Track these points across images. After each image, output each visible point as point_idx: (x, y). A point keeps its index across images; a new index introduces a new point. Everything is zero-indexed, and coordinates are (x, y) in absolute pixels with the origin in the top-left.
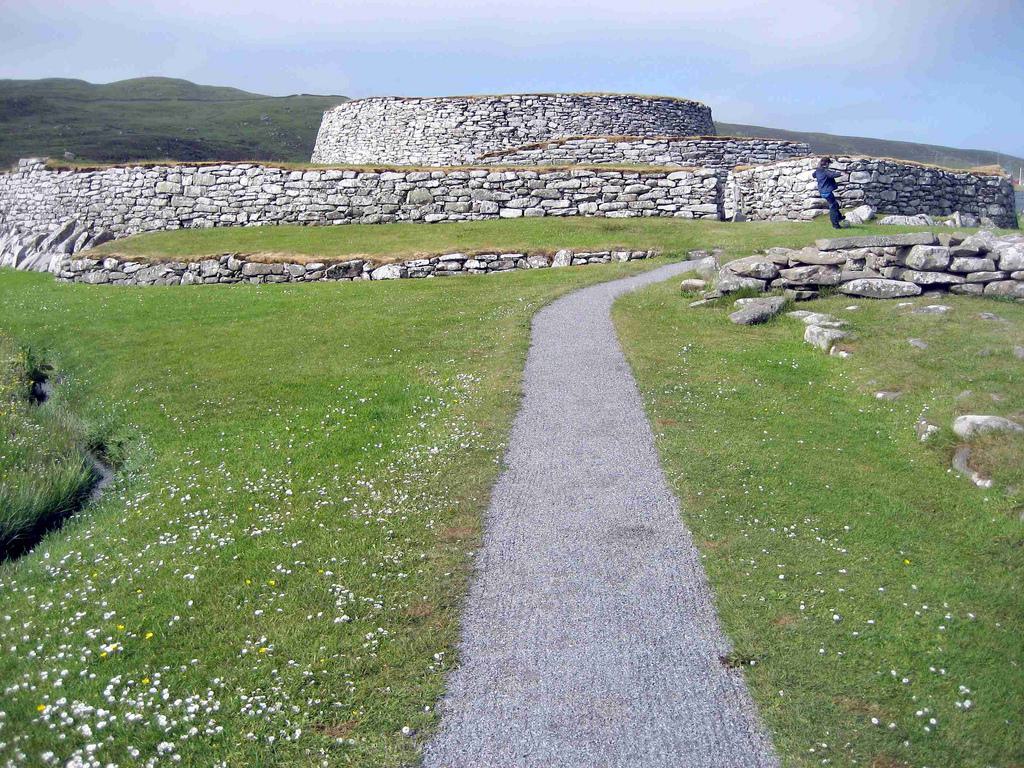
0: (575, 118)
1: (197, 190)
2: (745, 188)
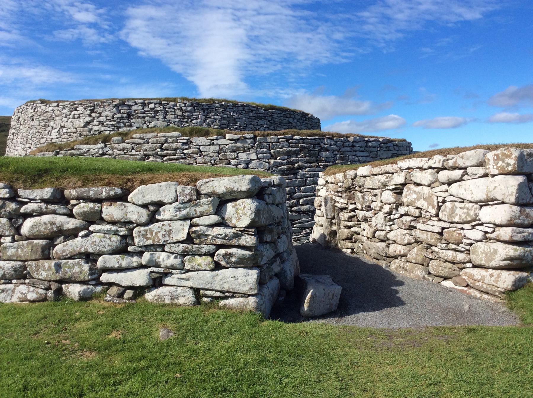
0: (193, 122)
2: (342, 201)
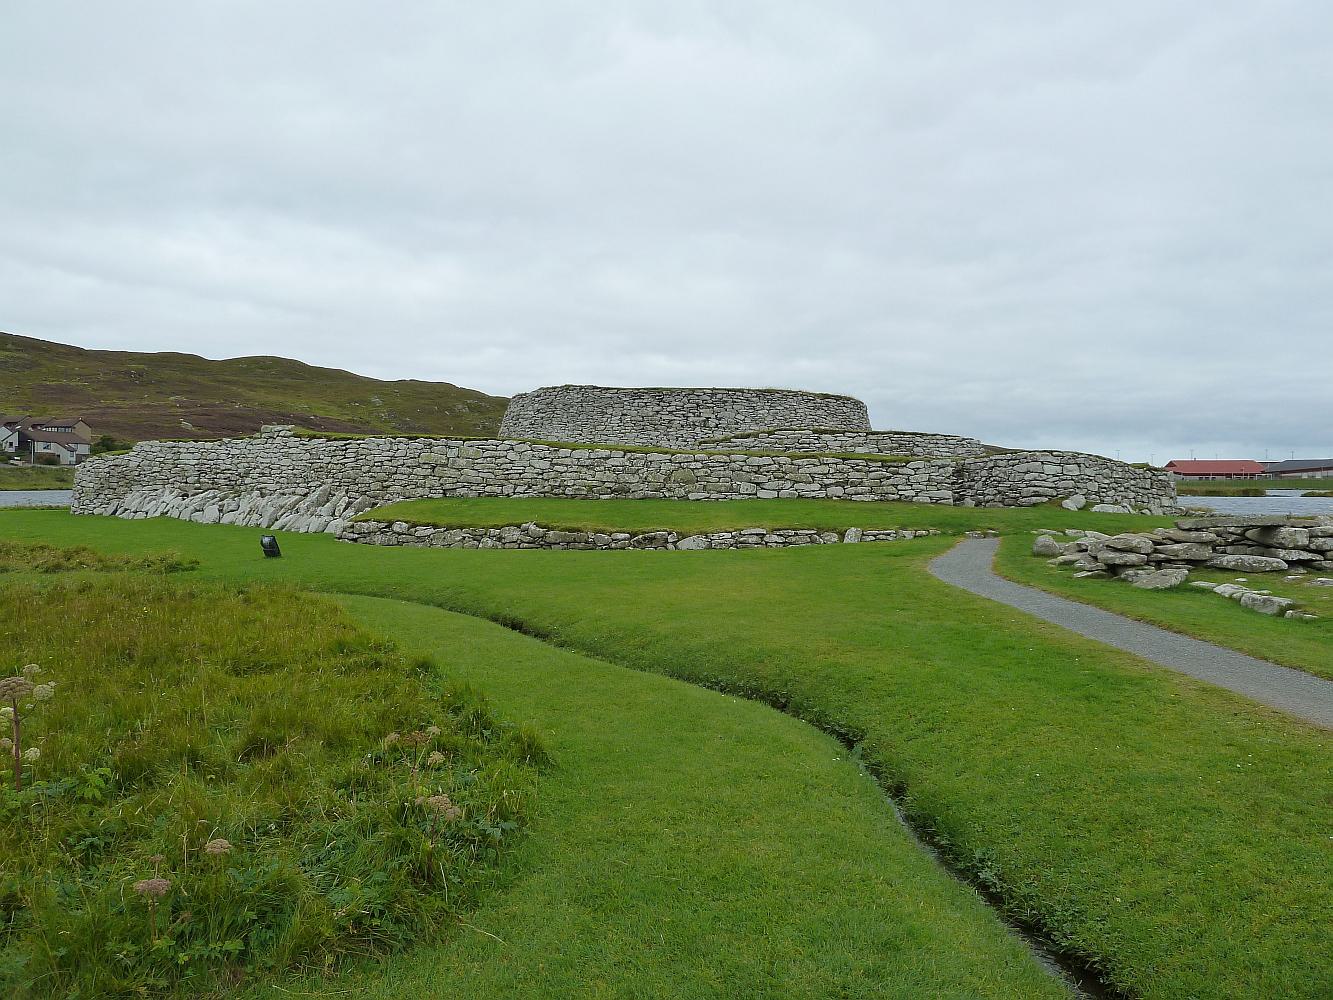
1: (462, 462)
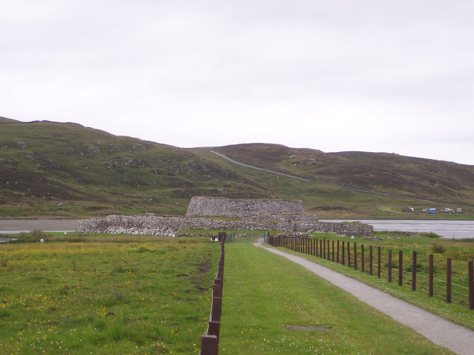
1: (194, 222)
